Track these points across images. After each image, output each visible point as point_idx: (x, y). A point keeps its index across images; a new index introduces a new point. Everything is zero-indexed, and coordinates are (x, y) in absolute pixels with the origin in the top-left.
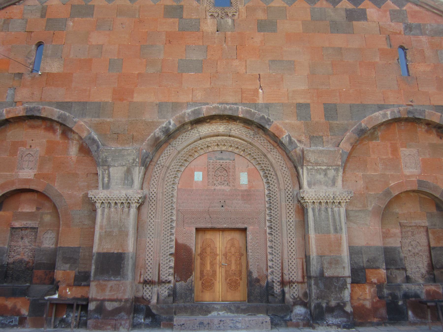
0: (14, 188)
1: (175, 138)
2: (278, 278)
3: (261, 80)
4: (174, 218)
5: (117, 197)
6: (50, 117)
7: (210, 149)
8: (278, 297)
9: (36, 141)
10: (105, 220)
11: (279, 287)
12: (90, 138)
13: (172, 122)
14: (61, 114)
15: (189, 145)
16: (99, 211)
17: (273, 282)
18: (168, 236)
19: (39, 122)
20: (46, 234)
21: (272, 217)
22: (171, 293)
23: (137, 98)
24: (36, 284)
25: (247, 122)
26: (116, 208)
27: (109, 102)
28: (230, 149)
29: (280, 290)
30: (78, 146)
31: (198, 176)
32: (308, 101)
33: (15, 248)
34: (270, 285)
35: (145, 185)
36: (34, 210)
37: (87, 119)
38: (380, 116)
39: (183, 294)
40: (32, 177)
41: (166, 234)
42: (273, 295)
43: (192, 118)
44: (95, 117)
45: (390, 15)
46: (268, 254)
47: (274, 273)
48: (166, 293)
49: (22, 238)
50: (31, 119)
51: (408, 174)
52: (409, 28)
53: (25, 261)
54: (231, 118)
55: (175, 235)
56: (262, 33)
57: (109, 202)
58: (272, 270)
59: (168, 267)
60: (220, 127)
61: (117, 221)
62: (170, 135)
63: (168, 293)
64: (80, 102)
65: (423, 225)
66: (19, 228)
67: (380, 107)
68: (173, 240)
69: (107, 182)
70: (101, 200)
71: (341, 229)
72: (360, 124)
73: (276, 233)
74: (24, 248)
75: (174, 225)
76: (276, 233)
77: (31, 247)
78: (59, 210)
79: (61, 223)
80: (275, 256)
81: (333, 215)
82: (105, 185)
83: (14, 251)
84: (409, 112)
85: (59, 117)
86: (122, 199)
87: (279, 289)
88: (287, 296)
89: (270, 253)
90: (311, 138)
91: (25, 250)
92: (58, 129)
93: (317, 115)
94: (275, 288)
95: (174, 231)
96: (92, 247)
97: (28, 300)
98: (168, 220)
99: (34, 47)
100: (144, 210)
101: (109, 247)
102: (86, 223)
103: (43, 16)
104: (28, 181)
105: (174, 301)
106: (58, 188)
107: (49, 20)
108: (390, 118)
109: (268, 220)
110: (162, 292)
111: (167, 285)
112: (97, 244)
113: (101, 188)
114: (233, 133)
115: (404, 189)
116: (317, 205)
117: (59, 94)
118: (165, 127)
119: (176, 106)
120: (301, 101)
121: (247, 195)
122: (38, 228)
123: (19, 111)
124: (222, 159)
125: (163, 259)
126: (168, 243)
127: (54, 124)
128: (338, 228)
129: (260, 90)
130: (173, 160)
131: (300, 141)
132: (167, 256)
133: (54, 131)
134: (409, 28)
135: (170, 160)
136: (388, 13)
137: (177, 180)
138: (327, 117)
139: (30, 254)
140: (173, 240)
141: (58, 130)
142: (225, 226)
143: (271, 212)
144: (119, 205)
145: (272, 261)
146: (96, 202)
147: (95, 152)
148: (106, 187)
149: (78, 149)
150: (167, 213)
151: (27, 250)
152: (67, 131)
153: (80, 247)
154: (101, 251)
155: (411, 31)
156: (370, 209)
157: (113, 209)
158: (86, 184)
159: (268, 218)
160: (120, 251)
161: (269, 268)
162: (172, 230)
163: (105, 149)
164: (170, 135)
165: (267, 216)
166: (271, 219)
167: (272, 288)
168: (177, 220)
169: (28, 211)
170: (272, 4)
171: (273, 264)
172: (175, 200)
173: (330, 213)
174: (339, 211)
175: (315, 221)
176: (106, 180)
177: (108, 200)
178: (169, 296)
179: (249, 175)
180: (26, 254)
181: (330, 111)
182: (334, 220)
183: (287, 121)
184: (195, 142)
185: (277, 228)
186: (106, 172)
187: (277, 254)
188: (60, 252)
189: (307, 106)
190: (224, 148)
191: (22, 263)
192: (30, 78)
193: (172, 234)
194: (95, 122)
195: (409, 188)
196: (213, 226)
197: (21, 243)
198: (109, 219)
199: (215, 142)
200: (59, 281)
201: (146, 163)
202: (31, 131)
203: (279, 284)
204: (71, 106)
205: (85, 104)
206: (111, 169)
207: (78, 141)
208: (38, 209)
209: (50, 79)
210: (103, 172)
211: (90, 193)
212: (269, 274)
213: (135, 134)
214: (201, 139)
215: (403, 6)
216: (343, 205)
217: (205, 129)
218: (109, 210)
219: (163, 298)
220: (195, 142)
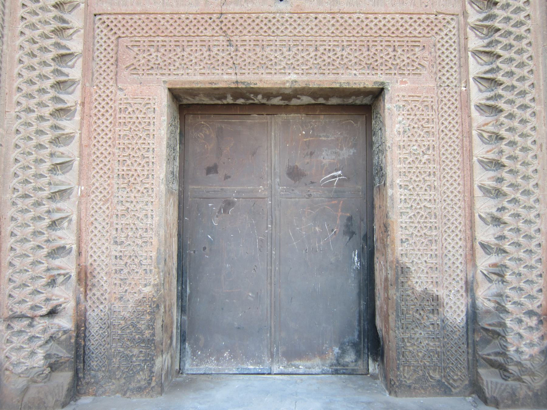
2: (531, 297)
8: (526, 378)
11: (535, 336)
17: (501, 309)
18: (41, 118)
21: (496, 36)
22: (65, 354)
29: (536, 350)
34: (485, 323)
39: (116, 361)
41: (29, 110)
42: (502, 368)
46: (478, 193)
47: (508, 277)
48: (39, 360)
55: (77, 117)
58: (494, 259)
59: (45, 251)
63: (47, 356)
68: (69, 138)
73: (519, 101)
75: (75, 72)
76: (519, 101)
80: (514, 201)
87: (531, 345)
89: (486, 191)
94: (510, 338)
95: (71, 99)
98: (45, 49)
109: (476, 53)
110: (14, 357)
111: (41, 324)
125: (19, 216)
126: (40, 146)
132: (38, 204)
140: (69, 138)
142: (293, 77)
143: (489, 17)
145: (497, 221)
150: (34, 19)
159: (475, 42)
161: (479, 251)
162: (62, 96)
165: (471, 34)
166: (489, 44)
167: (497, 334)
168: (89, 52)
171: (502, 238)
178: (54, 367)
185: (522, 79)
187: (527, 193)
193: (63, 112)
196: (240, 78)
203: (533, 322)
212: (480, 277)
219: (21, 383)
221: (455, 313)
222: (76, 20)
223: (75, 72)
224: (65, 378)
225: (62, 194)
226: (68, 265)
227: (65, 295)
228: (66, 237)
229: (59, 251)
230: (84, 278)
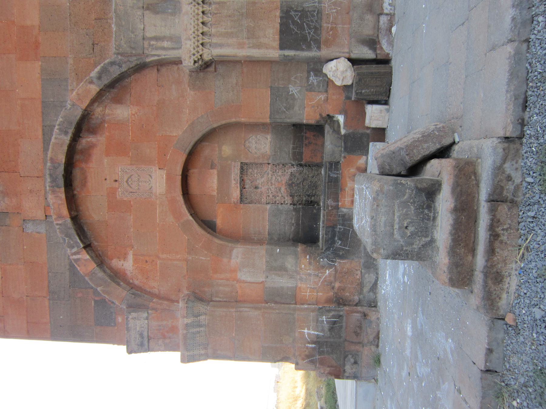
5: (193, 19)
6: (66, 148)
10: (230, 41)
12: (99, 78)
14: (60, 129)
16: (217, 52)
19: (77, 173)
20: (250, 150)
23: (33, 19)
24: (322, 157)
26: (211, 25)
27: (41, 66)
30: (114, 106)
33: (271, 196)
36: (215, 172)
40: (163, 173)
44: (67, 86)
49: (256, 188)
53: (290, 180)
57: (202, 34)
61: (232, 21)
64: (43, 113)
66: (241, 191)
69: (169, 43)
70: (198, 47)
74: (271, 183)
77: (270, 173)
78: (215, 125)
79: (234, 120)
82: (176, 46)
83: (275, 198)
85: (66, 133)
86: (196, 11)
91: (273, 181)
92: (87, 141)
97: (345, 157)
101: (271, 33)
102: (234, 81)
104: (169, 178)
106: (180, 132)
112: (266, 51)
113: (180, 51)
122: (242, 163)
123: (57, 200)
127: (79, 147)
133: (92, 146)
139: (280, 173)
141: (89, 140)
144: (206, 19)
146: (201, 56)
147: (121, 67)
148: (176, 41)
149: (118, 106)
151: (274, 178)
153: (271, 87)
154: (276, 44)
157: (213, 30)
158: (174, 86)
160: (278, 13)
163: (116, 41)
169: (215, 181)
176: (166, 44)
177: (198, 36)
180: (280, 180)
186: (153, 45)
188: (277, 117)
191: (293, 183)
192: (6, 199)
194: (75, 83)
197: (263, 189)
200: (321, 115)
202: (91, 183)
204: (49, 126)
205: (45, 105)
206: (148, 35)
207: (106, 107)
208: (212, 167)
210: (153, 49)
211: (186, 62)
213: (93, 16)
218: (214, 35)
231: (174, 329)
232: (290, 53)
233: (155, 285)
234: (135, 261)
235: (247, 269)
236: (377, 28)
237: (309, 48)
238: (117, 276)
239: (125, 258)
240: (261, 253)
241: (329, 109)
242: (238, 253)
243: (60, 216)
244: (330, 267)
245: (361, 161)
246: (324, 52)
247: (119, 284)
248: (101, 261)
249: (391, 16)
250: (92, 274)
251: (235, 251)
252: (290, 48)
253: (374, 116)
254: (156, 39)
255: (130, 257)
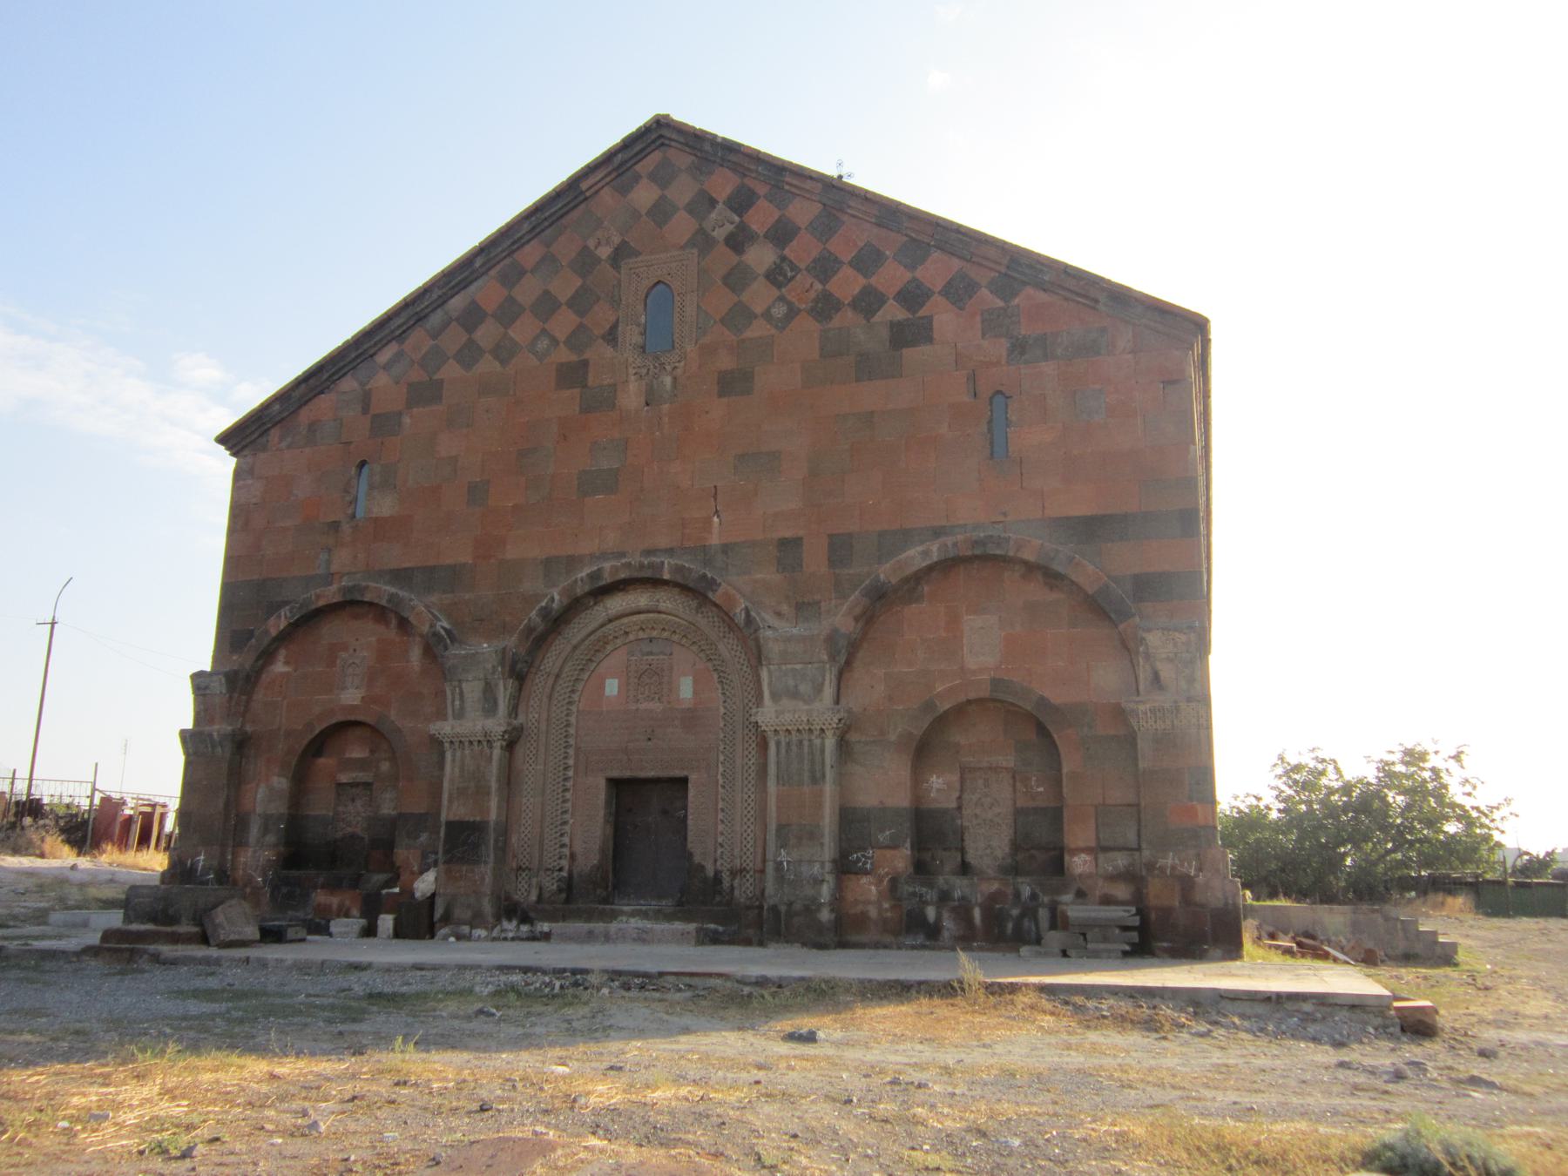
0: (334, 721)
1: (568, 622)
3: (719, 497)
4: (571, 762)
7: (631, 637)
9: (360, 641)
13: (557, 597)
15: (593, 632)
16: (448, 756)
23: (512, 553)
25: (684, 588)
28: (666, 634)
31: (612, 687)
32: (801, 533)
35: (521, 708)
37: (434, 598)
38: (915, 556)
43: (587, 588)
45: (983, 322)
49: (353, 800)
50: (350, 605)
51: (974, 667)
52: (1019, 348)
54: (655, 582)
56: (725, 400)
60: (640, 598)
62: (557, 622)
65: (1004, 764)
67: (937, 532)
71: (824, 776)
72: (878, 576)
75: (570, 773)
81: (812, 753)
84: (976, 543)
85: (389, 601)
88: (737, 893)
90: (800, 607)
93: (815, 560)
95: (569, 784)
96: (439, 814)
99: (353, 471)
100: (520, 750)
103: (365, 410)
104: (353, 708)
105: (568, 901)
107: (376, 416)
108: (935, 559)
114: (663, 606)
115: (962, 698)
116: (783, 738)
117: (393, 556)
118: (545, 608)
119: (572, 562)
120: (788, 534)
121: (691, 718)
123: (331, 594)
124: (651, 653)
128: (818, 775)
129: (716, 519)
130: (565, 661)
131: (779, 614)
133: (387, 624)
134: (1019, 348)
135: (560, 661)
136: (978, 319)
137: (576, 697)
138: (832, 563)
152: (404, 624)
154: (451, 818)
155: (1022, 353)
156: (893, 737)
164: (557, 622)
168: (576, 766)
170: (748, 334)
172: (572, 731)
173: (806, 750)
174: (823, 745)
175: (778, 763)
178: (560, 890)
179: (695, 682)
181: (840, 549)
182: (812, 762)
183: (759, 576)
184: (602, 626)
189: (796, 542)
190: (655, 634)
193: (567, 790)
195: (972, 695)
198: (462, 769)
199: (635, 624)
201: (519, 672)
205: (432, 569)
208: (372, 752)
209: (381, 528)
214: (610, 621)
215: (1015, 294)
216: (829, 733)
217: (616, 604)
220: (602, 626)
221: (710, 873)
222: (571, 752)
223: (570, 773)
224: (564, 895)
225: (565, 823)
226: (566, 851)
227: (565, 863)
228: (566, 840)
229: (563, 846)
230: (573, 857)
231: (211, 721)
232: (442, 834)
233: (260, 695)
234: (282, 675)
235: (266, 793)
236: (460, 923)
237: (446, 852)
238: (267, 656)
239: (287, 663)
240: (279, 808)
241: (404, 877)
242: (281, 783)
243: (318, 597)
244: (264, 881)
245: (355, 912)
246: (441, 866)
247: (257, 660)
248: (284, 637)
249: (468, 938)
250: (266, 632)
251: (284, 780)
252: (447, 834)
253: (386, 922)
254: (461, 694)
255: (286, 669)
